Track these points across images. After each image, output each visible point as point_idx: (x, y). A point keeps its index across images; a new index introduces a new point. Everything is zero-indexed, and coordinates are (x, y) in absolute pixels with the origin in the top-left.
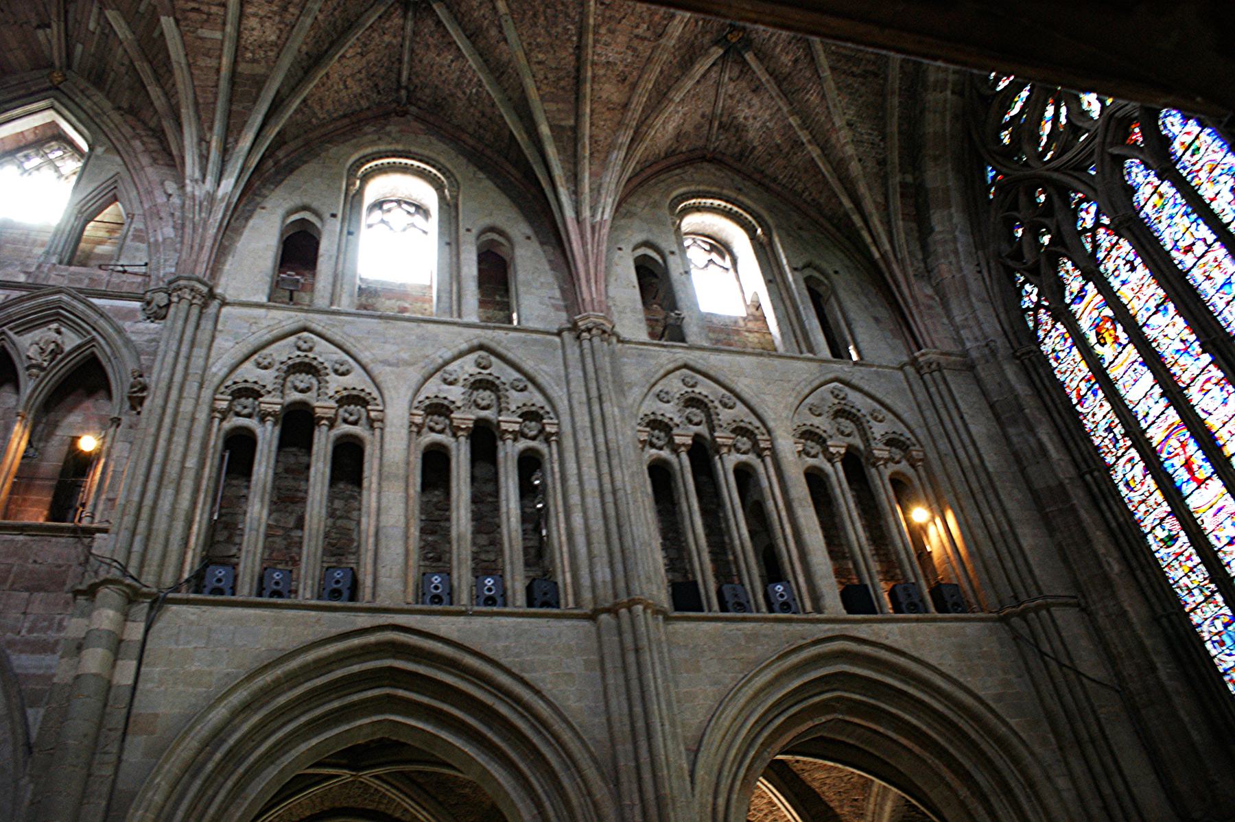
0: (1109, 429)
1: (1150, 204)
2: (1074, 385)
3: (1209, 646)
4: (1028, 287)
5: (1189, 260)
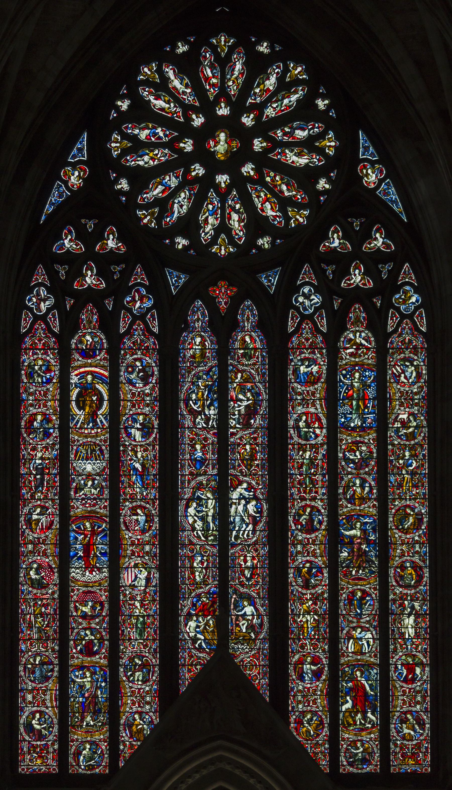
0: (41, 471)
1: (191, 352)
2: (32, 410)
3: (21, 668)
4: (43, 292)
5: (188, 423)
